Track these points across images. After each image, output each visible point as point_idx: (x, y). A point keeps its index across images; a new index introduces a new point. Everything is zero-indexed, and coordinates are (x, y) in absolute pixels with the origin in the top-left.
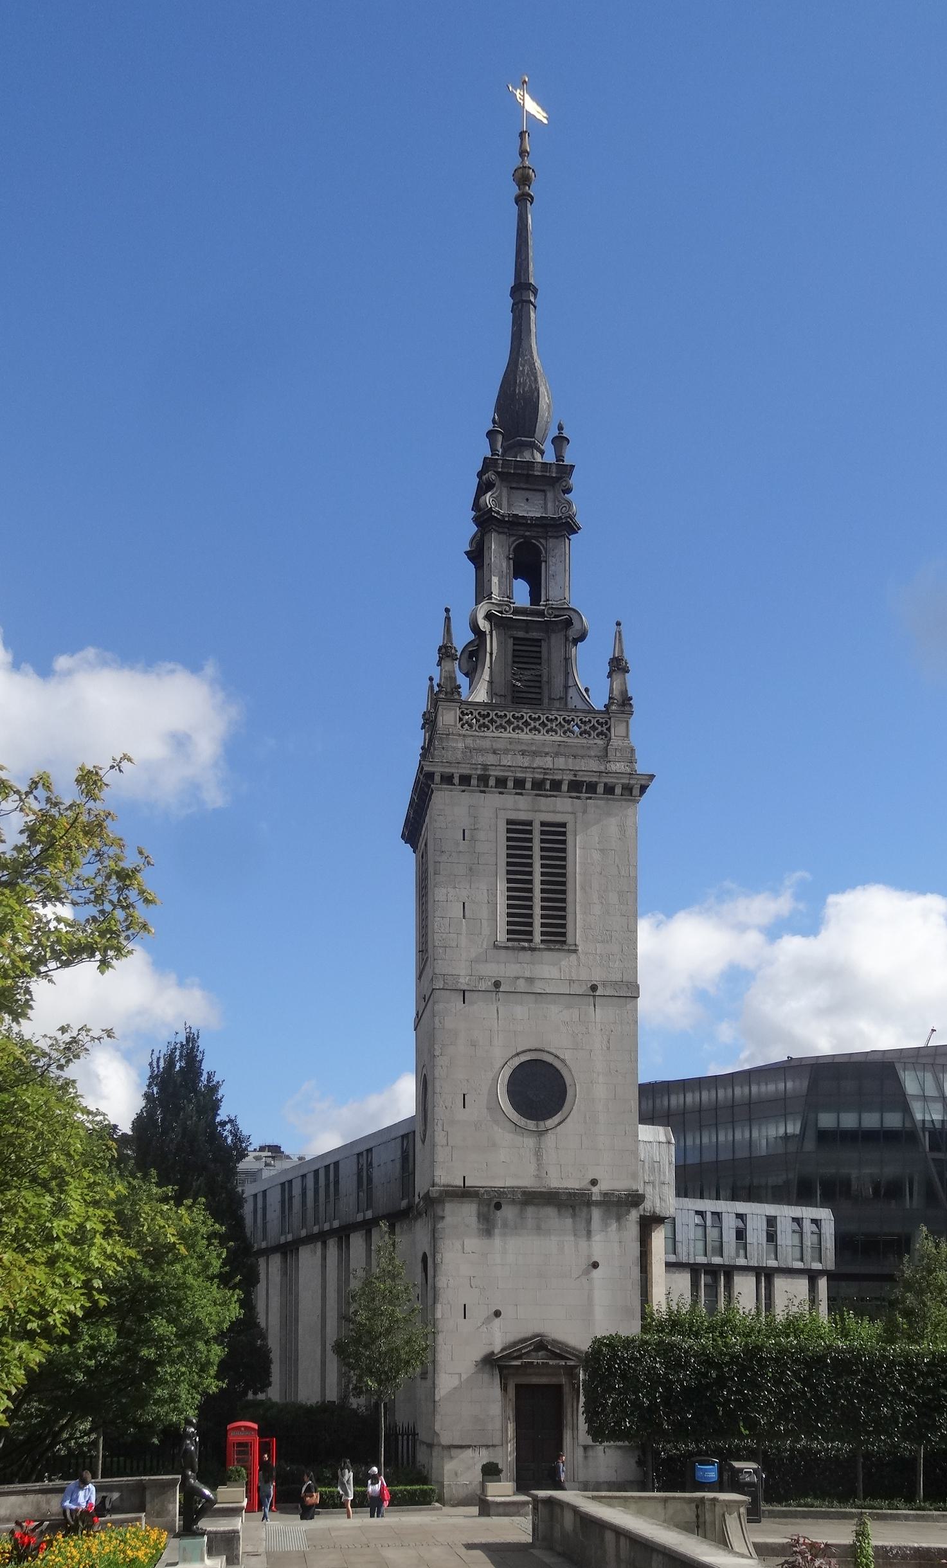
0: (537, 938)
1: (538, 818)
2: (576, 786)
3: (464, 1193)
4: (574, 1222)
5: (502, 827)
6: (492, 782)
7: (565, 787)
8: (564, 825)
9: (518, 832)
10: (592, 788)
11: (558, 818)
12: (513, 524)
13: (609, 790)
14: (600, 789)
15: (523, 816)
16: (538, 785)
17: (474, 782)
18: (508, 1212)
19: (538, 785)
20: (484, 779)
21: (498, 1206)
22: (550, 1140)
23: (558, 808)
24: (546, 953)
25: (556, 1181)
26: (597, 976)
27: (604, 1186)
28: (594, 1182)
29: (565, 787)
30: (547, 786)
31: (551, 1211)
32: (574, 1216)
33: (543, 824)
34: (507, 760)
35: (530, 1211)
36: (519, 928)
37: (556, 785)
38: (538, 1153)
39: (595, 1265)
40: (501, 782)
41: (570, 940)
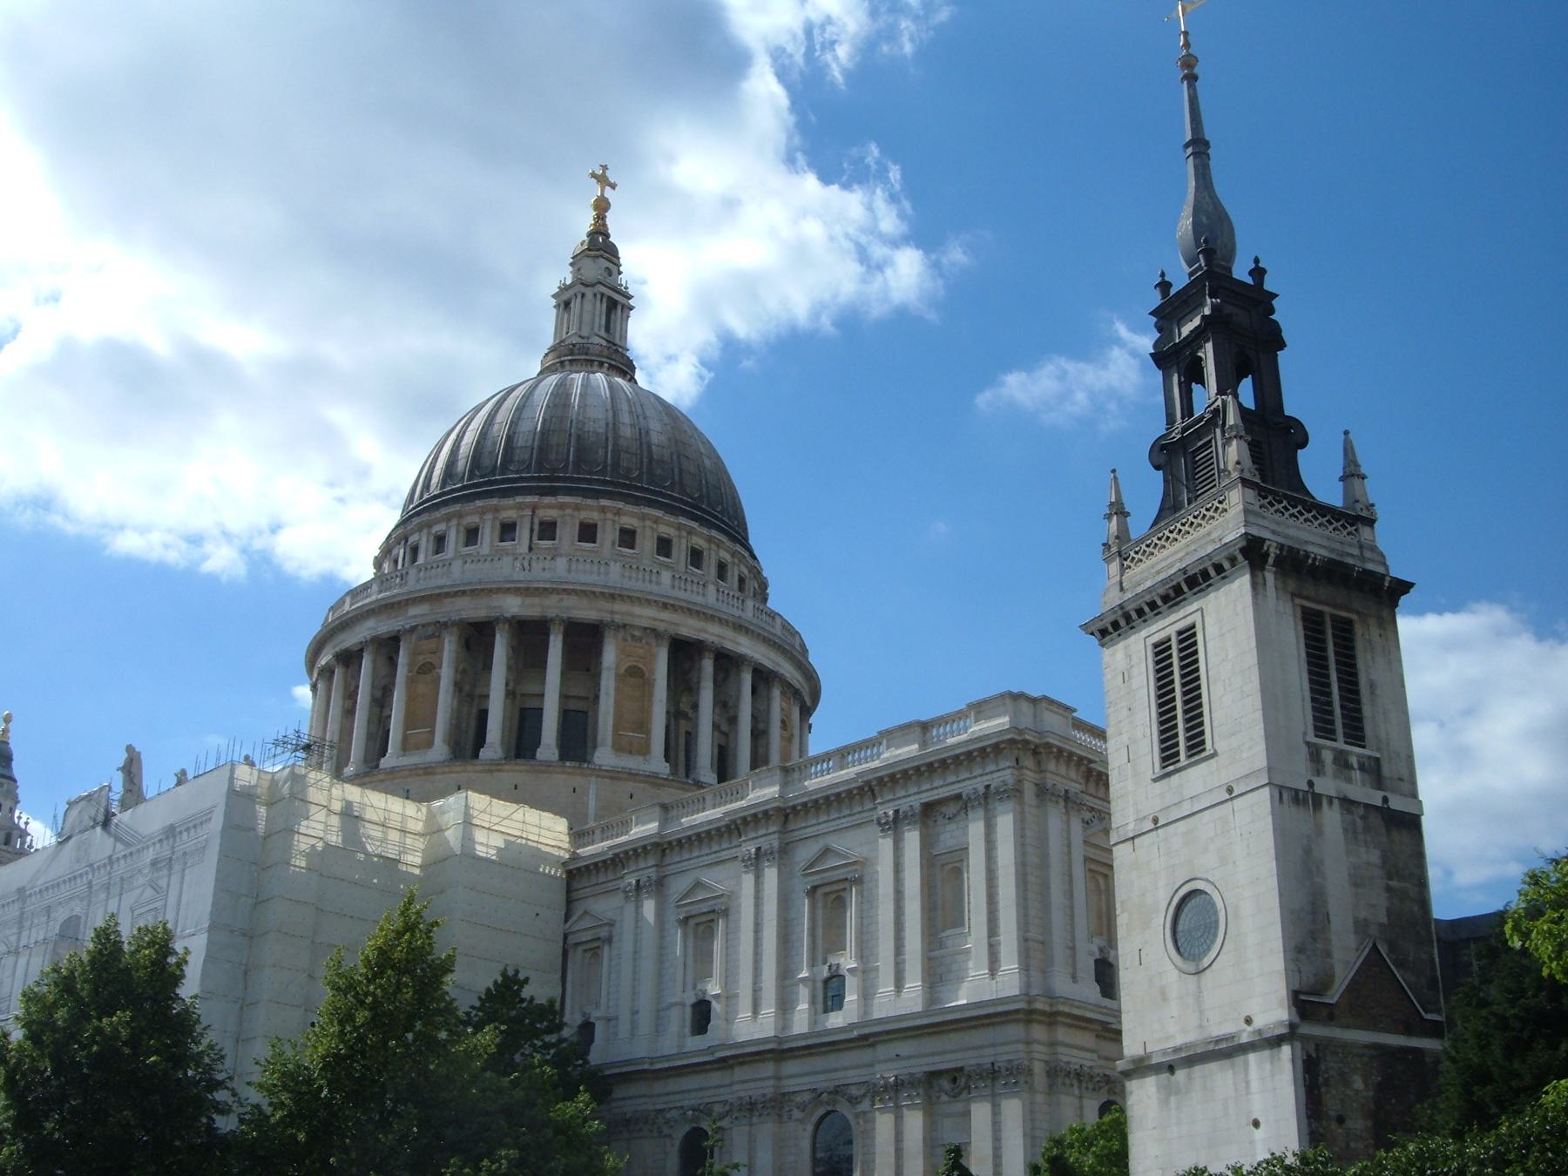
31: (1213, 1067)
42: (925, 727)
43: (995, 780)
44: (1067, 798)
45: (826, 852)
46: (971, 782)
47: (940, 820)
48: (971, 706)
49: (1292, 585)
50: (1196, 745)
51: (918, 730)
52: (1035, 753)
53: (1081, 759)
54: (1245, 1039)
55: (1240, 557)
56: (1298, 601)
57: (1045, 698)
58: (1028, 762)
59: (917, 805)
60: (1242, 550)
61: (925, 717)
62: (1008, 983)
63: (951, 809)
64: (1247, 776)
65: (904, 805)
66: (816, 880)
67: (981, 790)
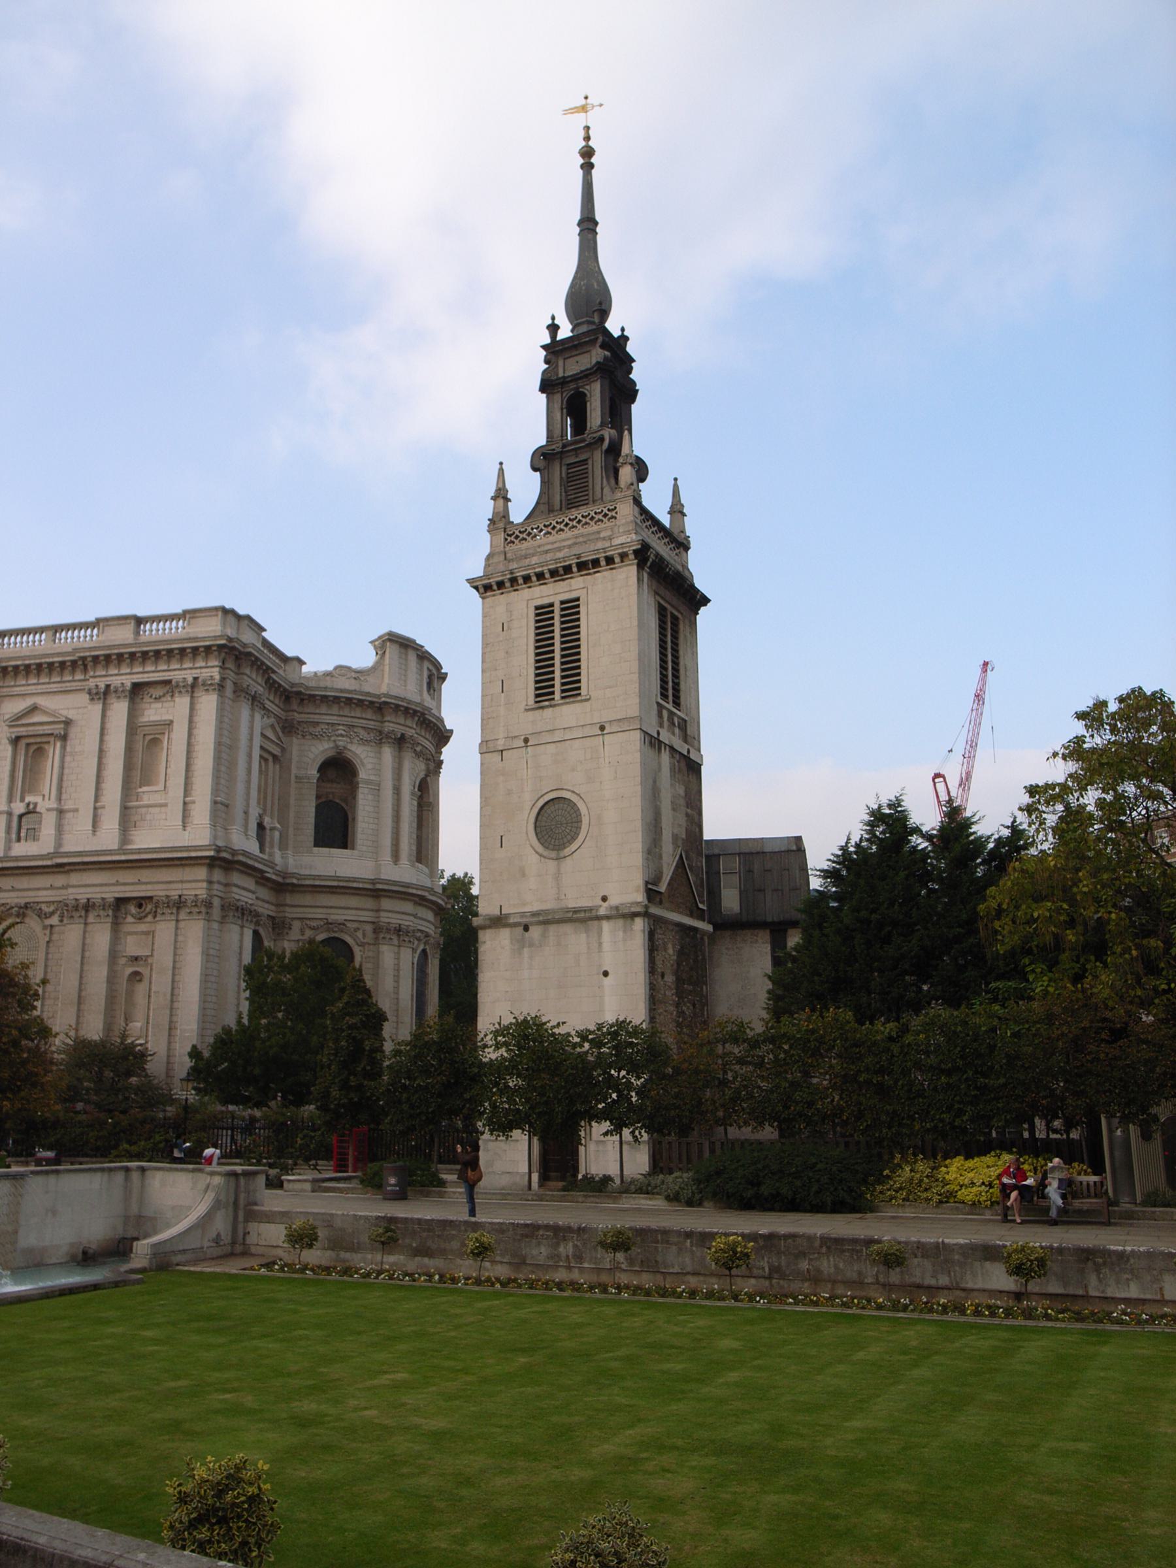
0: (557, 696)
1: (556, 601)
2: (582, 566)
3: (498, 921)
4: (588, 936)
5: (532, 612)
6: (521, 581)
7: (575, 569)
8: (578, 599)
9: (543, 613)
10: (596, 563)
11: (574, 595)
12: (564, 382)
13: (610, 560)
14: (603, 563)
15: (546, 601)
16: (554, 573)
17: (508, 584)
18: (535, 932)
19: (554, 573)
20: (513, 581)
21: (526, 928)
22: (568, 864)
23: (574, 586)
24: (564, 708)
25: (575, 899)
26: (605, 716)
27: (614, 901)
28: (604, 899)
29: (575, 569)
30: (562, 572)
31: (567, 928)
32: (587, 931)
33: (562, 603)
34: (535, 560)
35: (552, 929)
36: (543, 693)
37: (568, 569)
38: (558, 876)
39: (606, 974)
40: (527, 579)
41: (583, 691)
42: (139, 621)
43: (204, 674)
44: (254, 698)
45: (34, 709)
46: (181, 672)
47: (147, 699)
48: (185, 612)
49: (655, 584)
50: (572, 689)
51: (133, 622)
52: (237, 658)
53: (268, 668)
54: (602, 912)
55: (632, 557)
56: (658, 598)
57: (249, 618)
58: (230, 664)
59: (128, 686)
60: (636, 552)
61: (141, 613)
62: (198, 835)
63: (157, 692)
64: (619, 720)
65: (116, 681)
66: (22, 731)
67: (190, 680)
